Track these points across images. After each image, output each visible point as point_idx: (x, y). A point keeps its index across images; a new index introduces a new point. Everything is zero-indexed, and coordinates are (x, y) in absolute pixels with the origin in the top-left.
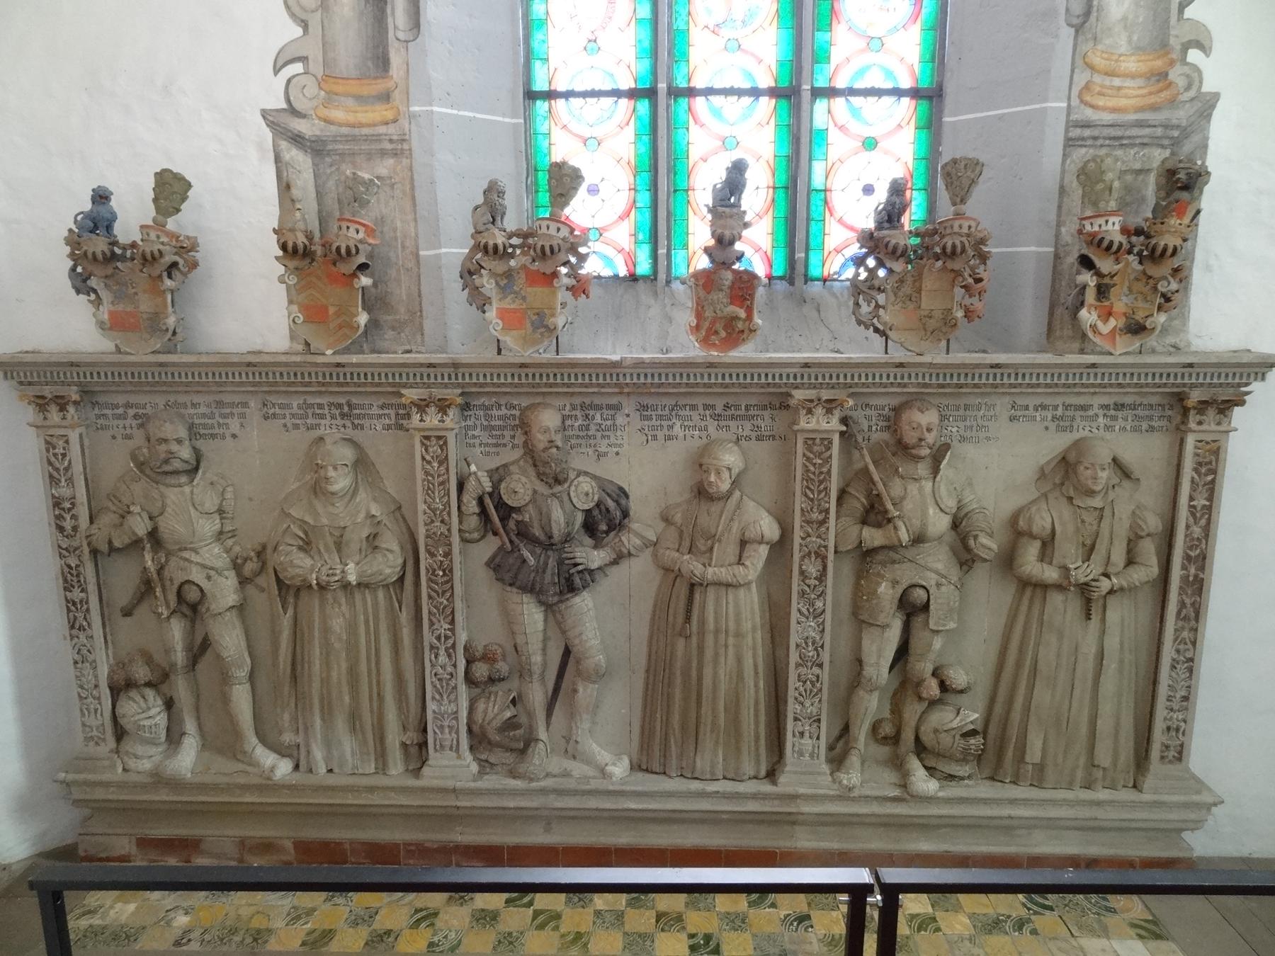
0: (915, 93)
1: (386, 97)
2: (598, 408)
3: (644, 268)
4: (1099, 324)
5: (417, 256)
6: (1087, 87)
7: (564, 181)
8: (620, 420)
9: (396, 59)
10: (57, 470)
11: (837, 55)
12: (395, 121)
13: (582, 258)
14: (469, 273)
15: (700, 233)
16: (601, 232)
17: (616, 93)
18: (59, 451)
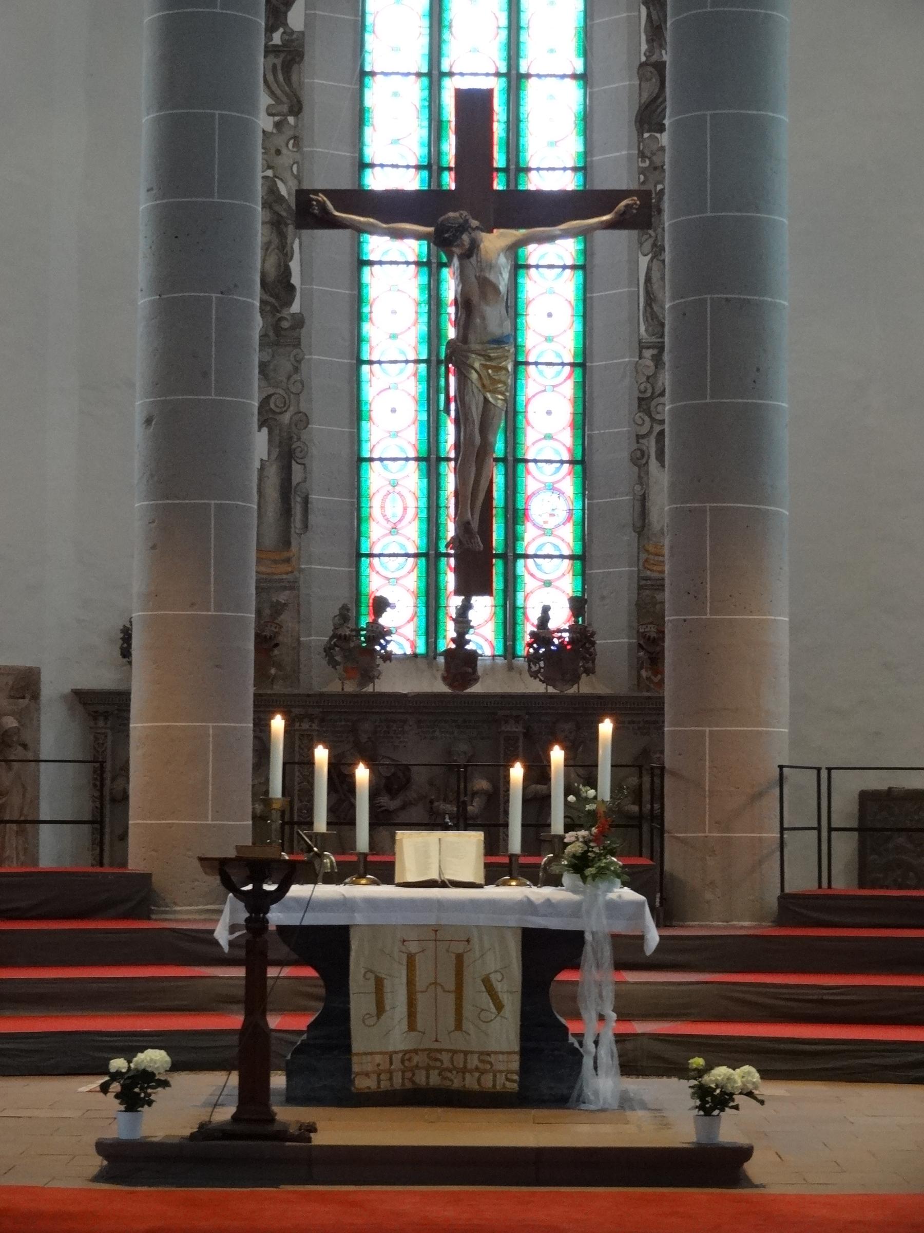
0: (572, 557)
1: (288, 561)
2: (394, 721)
3: (421, 649)
4: (653, 677)
5: (298, 640)
6: (646, 561)
7: (380, 605)
8: (406, 728)
9: (294, 542)
10: (98, 752)
11: (528, 537)
12: (292, 572)
13: (388, 642)
14: (328, 650)
15: (450, 630)
16: (397, 628)
17: (407, 555)
18: (101, 742)
